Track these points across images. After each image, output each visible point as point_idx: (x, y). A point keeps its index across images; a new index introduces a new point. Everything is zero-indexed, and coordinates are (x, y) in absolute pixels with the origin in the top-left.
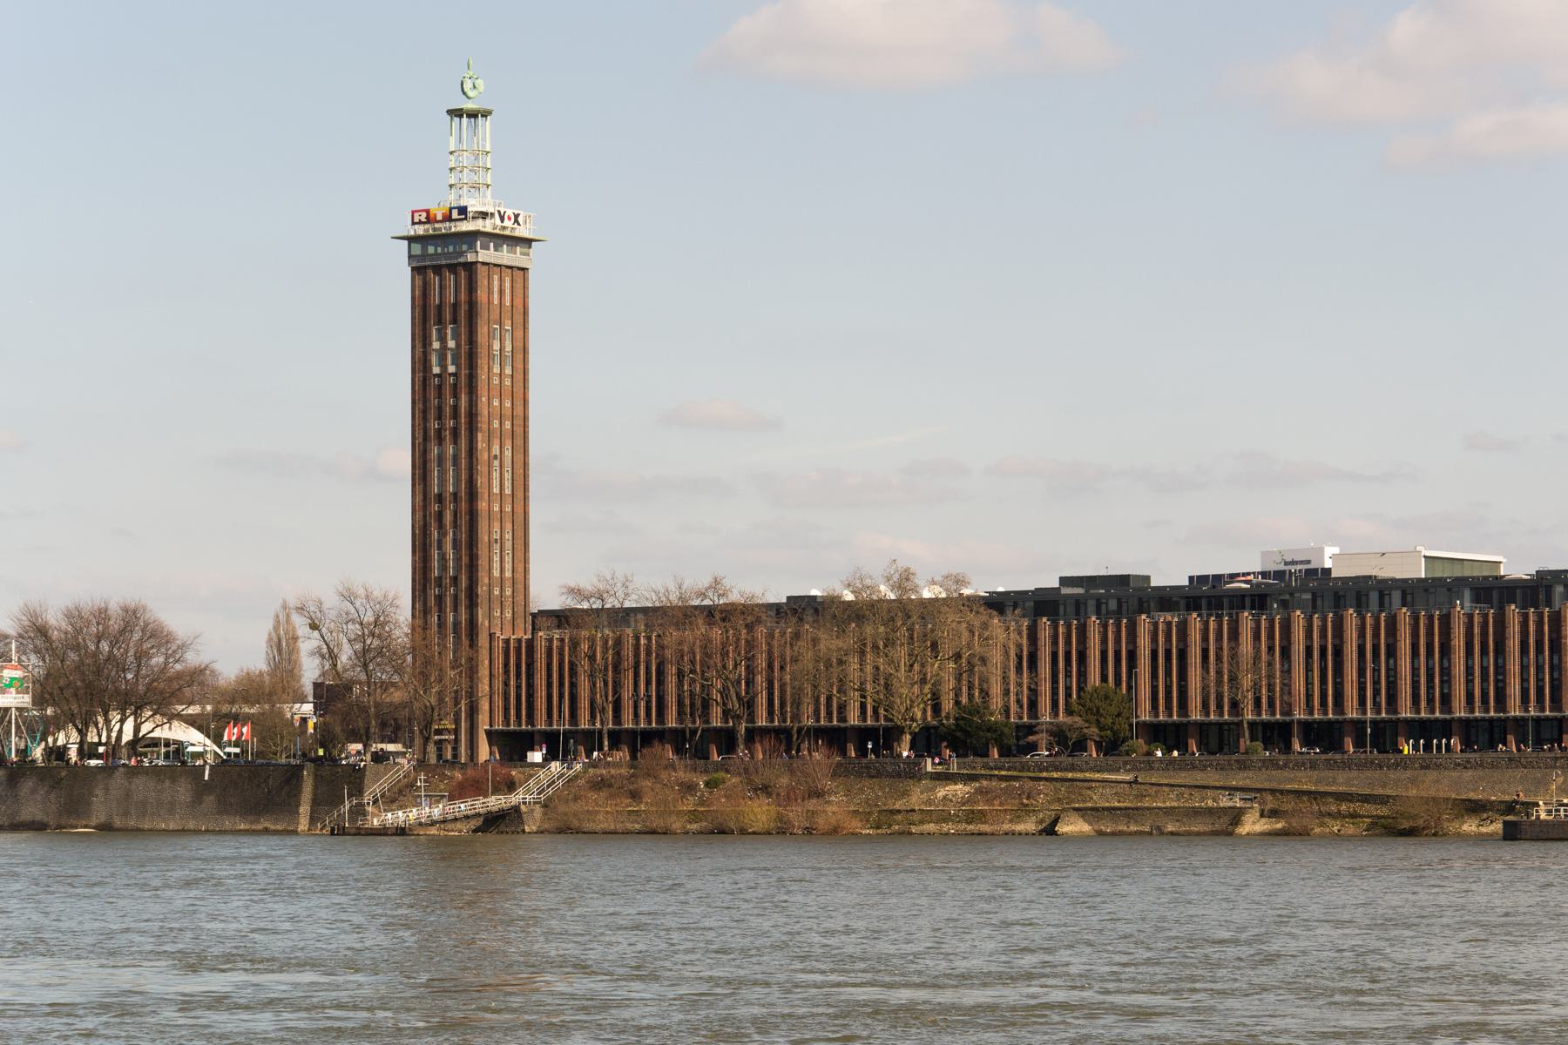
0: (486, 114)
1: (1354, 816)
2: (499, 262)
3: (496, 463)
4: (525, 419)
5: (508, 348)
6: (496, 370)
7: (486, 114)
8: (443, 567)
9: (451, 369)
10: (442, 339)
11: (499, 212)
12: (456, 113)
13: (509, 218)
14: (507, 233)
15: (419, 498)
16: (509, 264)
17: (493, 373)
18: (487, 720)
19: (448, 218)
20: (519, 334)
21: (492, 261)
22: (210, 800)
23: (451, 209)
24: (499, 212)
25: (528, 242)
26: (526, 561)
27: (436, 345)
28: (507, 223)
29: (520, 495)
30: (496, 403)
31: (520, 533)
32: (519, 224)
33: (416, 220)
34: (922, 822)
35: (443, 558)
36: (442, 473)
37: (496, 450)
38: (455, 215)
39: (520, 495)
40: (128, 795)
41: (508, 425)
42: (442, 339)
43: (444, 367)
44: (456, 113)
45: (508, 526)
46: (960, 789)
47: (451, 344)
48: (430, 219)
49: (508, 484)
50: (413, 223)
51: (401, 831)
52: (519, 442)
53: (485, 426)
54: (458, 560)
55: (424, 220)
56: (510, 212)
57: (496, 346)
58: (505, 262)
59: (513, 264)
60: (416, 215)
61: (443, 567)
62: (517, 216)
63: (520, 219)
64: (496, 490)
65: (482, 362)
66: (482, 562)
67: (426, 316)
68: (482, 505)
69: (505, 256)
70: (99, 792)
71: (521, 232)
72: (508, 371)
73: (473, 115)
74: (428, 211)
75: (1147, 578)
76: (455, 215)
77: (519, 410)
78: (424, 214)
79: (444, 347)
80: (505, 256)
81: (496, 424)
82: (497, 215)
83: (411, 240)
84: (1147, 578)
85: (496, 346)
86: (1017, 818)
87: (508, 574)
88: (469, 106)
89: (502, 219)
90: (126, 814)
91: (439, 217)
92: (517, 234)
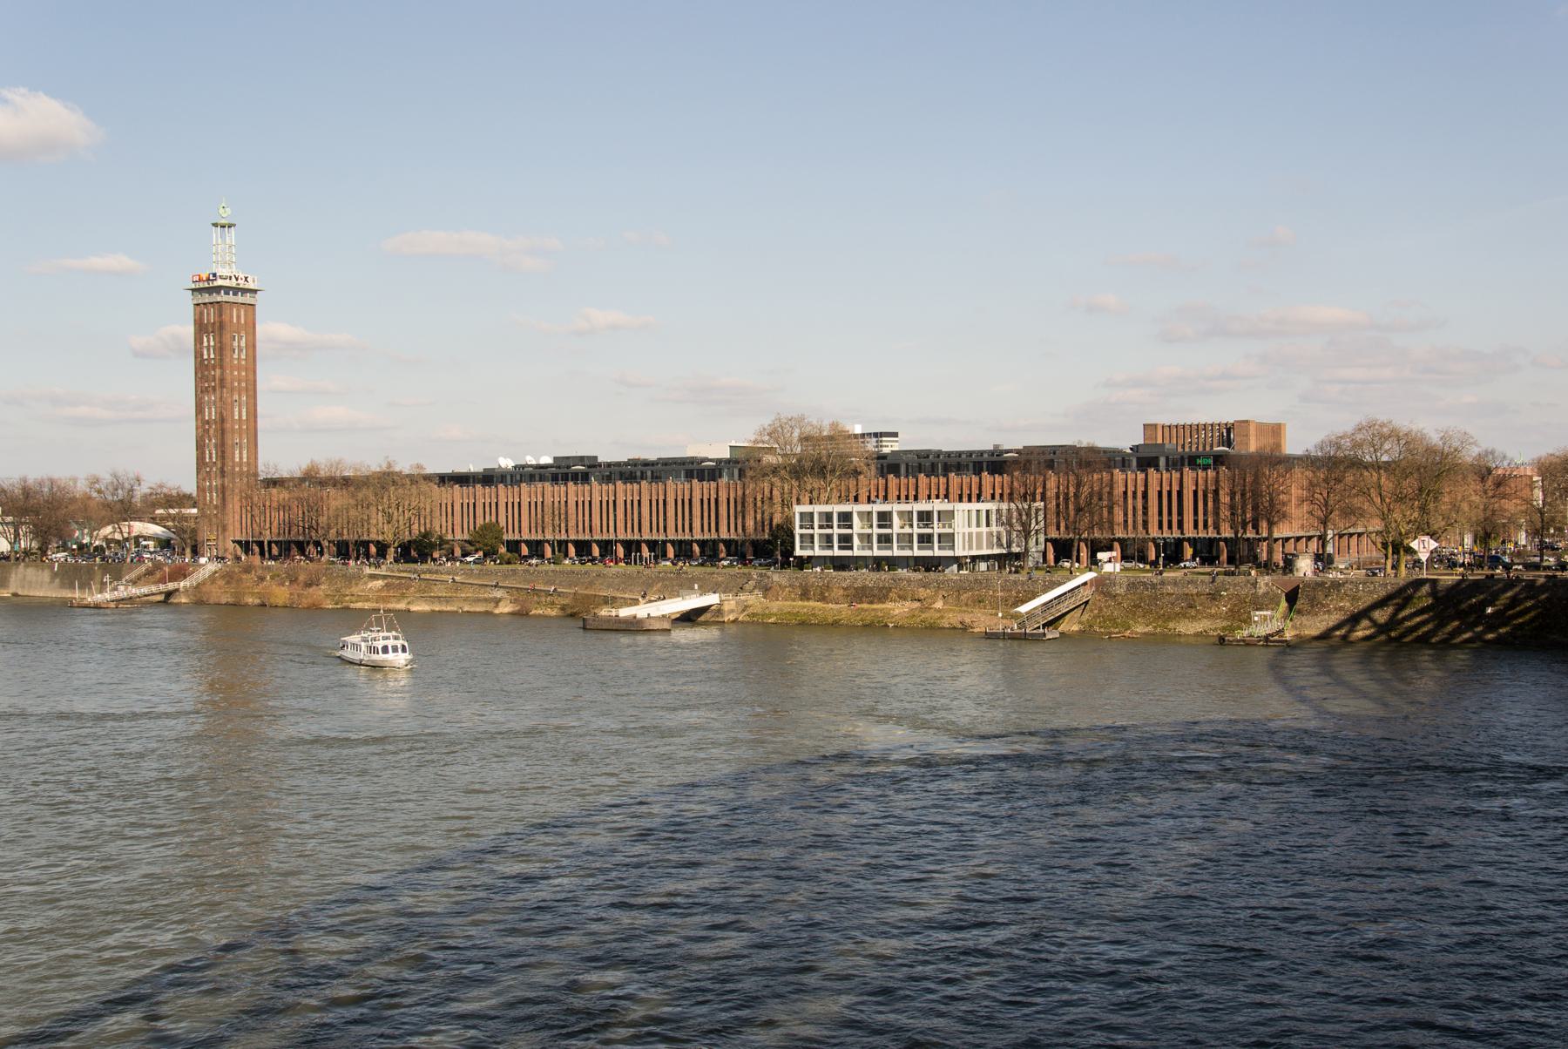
0: (234, 225)
1: (553, 603)
4: (255, 381)
7: (234, 225)
8: (211, 458)
9: (212, 356)
10: (208, 341)
12: (215, 225)
15: (199, 421)
17: (238, 356)
18: (232, 534)
19: (208, 280)
20: (251, 337)
22: (57, 580)
25: (255, 291)
26: (256, 453)
27: (205, 344)
28: (240, 281)
29: (252, 419)
30: (236, 373)
31: (252, 439)
34: (357, 602)
35: (211, 454)
36: (210, 409)
37: (236, 397)
40: (25, 576)
41: (243, 384)
42: (208, 341)
43: (209, 355)
44: (215, 225)
45: (245, 436)
46: (380, 583)
47: (212, 343)
49: (244, 414)
51: (97, 607)
52: (251, 393)
53: (228, 385)
54: (217, 453)
56: (242, 276)
57: (236, 344)
58: (240, 301)
61: (211, 458)
62: (246, 278)
64: (237, 417)
65: (227, 353)
66: (228, 454)
67: (201, 328)
68: (228, 426)
69: (240, 298)
70: (13, 575)
71: (251, 286)
72: (243, 357)
75: (596, 457)
77: (251, 377)
79: (209, 345)
80: (248, 299)
81: (236, 384)
82: (233, 278)
83: (193, 290)
84: (596, 457)
85: (236, 344)
86: (398, 601)
87: (245, 460)
88: (223, 222)
89: (237, 279)
90: (23, 587)
92: (246, 287)
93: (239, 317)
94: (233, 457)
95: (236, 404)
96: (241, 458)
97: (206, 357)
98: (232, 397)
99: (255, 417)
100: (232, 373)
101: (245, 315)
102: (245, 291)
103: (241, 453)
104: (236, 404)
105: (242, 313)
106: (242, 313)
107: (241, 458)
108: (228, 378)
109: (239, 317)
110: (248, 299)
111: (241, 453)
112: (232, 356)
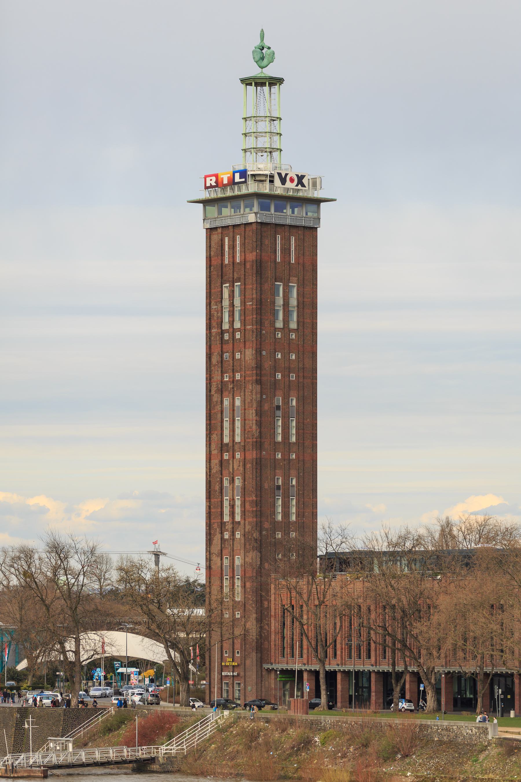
2: (281, 222)
5: (293, 302)
6: (279, 324)
11: (280, 174)
13: (292, 180)
14: (291, 193)
16: (293, 223)
19: (232, 183)
21: (273, 221)
23: (234, 173)
25: (317, 202)
28: (288, 184)
32: (303, 185)
33: (208, 185)
37: (279, 400)
38: (237, 179)
39: (308, 443)
41: (293, 377)
43: (232, 322)
45: (293, 472)
48: (218, 184)
50: (206, 188)
55: (214, 184)
57: (280, 301)
59: (298, 224)
60: (208, 179)
61: (232, 514)
72: (293, 325)
74: (216, 176)
76: (237, 179)
78: (214, 179)
83: (206, 202)
89: (283, 181)
91: (225, 182)
93: (286, 251)
94: (274, 513)
96: (286, 514)
97: (226, 326)
103: (286, 506)
104: (279, 413)
107: (286, 514)
108: (267, 364)
109: (286, 251)
111: (286, 506)
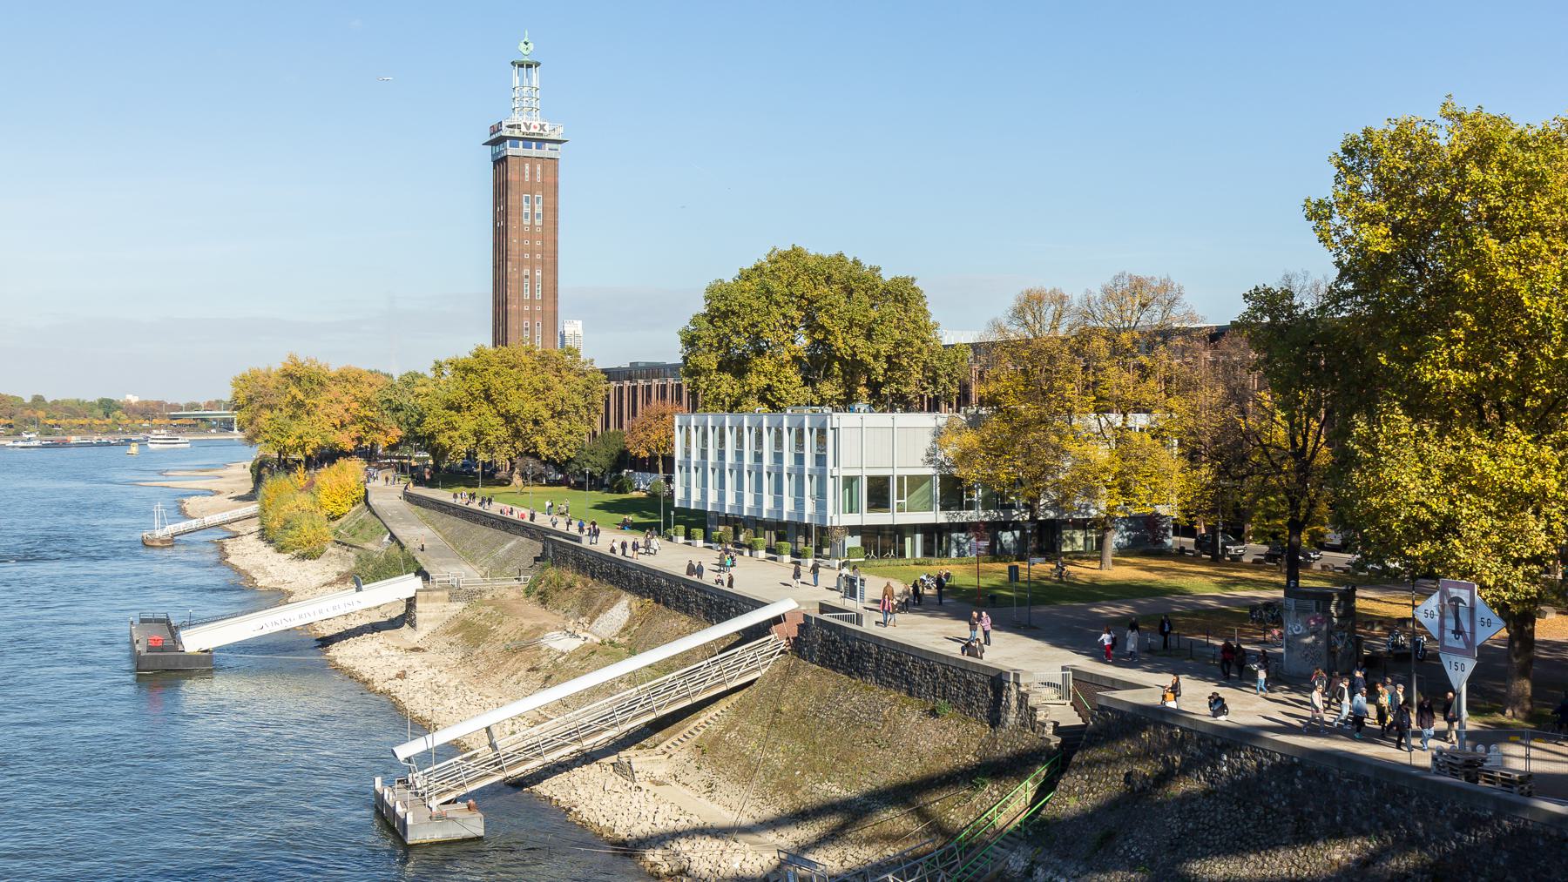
0: (538, 64)
3: (527, 282)
4: (555, 252)
7: (538, 64)
11: (525, 124)
24: (525, 124)
37: (526, 271)
41: (538, 256)
45: (538, 320)
52: (549, 266)
58: (534, 155)
63: (546, 128)
69: (534, 151)
72: (538, 222)
73: (529, 66)
77: (550, 246)
81: (527, 256)
89: (528, 127)
93: (532, 174)
95: (527, 282)
98: (520, 271)
99: (555, 296)
100: (520, 242)
101: (543, 171)
102: (541, 142)
105: (539, 168)
106: (539, 168)
109: (532, 174)
110: (547, 151)
112: (521, 222)
